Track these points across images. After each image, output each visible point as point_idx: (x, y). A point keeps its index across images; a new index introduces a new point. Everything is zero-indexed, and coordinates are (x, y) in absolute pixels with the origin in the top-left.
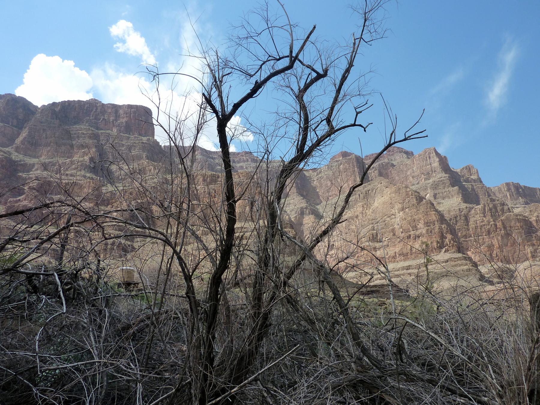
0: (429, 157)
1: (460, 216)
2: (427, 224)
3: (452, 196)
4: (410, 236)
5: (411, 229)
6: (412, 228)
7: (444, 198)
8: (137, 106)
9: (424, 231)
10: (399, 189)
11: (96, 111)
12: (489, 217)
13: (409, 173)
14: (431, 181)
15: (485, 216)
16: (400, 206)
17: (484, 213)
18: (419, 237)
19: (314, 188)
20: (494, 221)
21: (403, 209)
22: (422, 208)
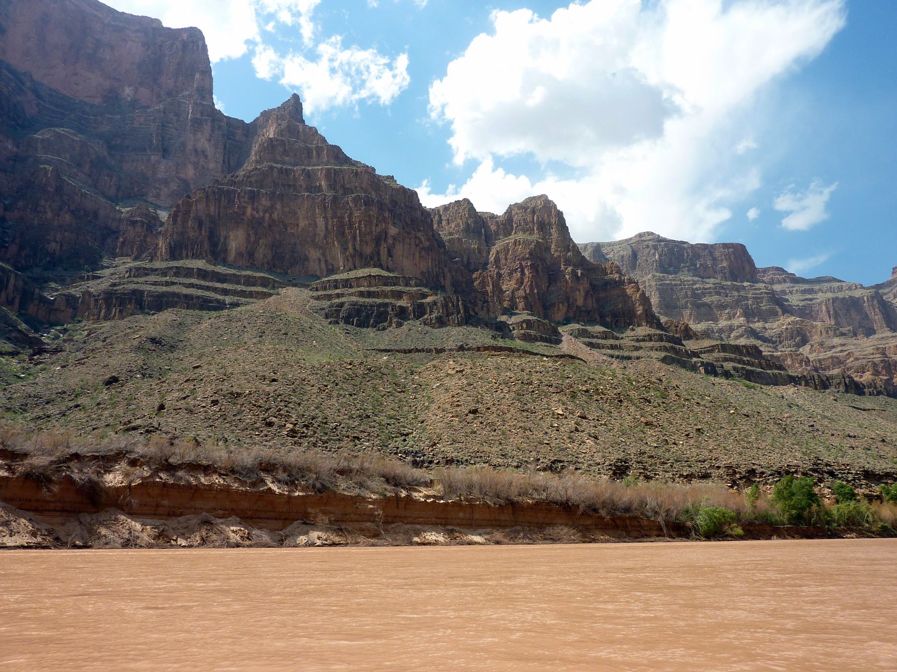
8: (732, 244)
11: (688, 255)
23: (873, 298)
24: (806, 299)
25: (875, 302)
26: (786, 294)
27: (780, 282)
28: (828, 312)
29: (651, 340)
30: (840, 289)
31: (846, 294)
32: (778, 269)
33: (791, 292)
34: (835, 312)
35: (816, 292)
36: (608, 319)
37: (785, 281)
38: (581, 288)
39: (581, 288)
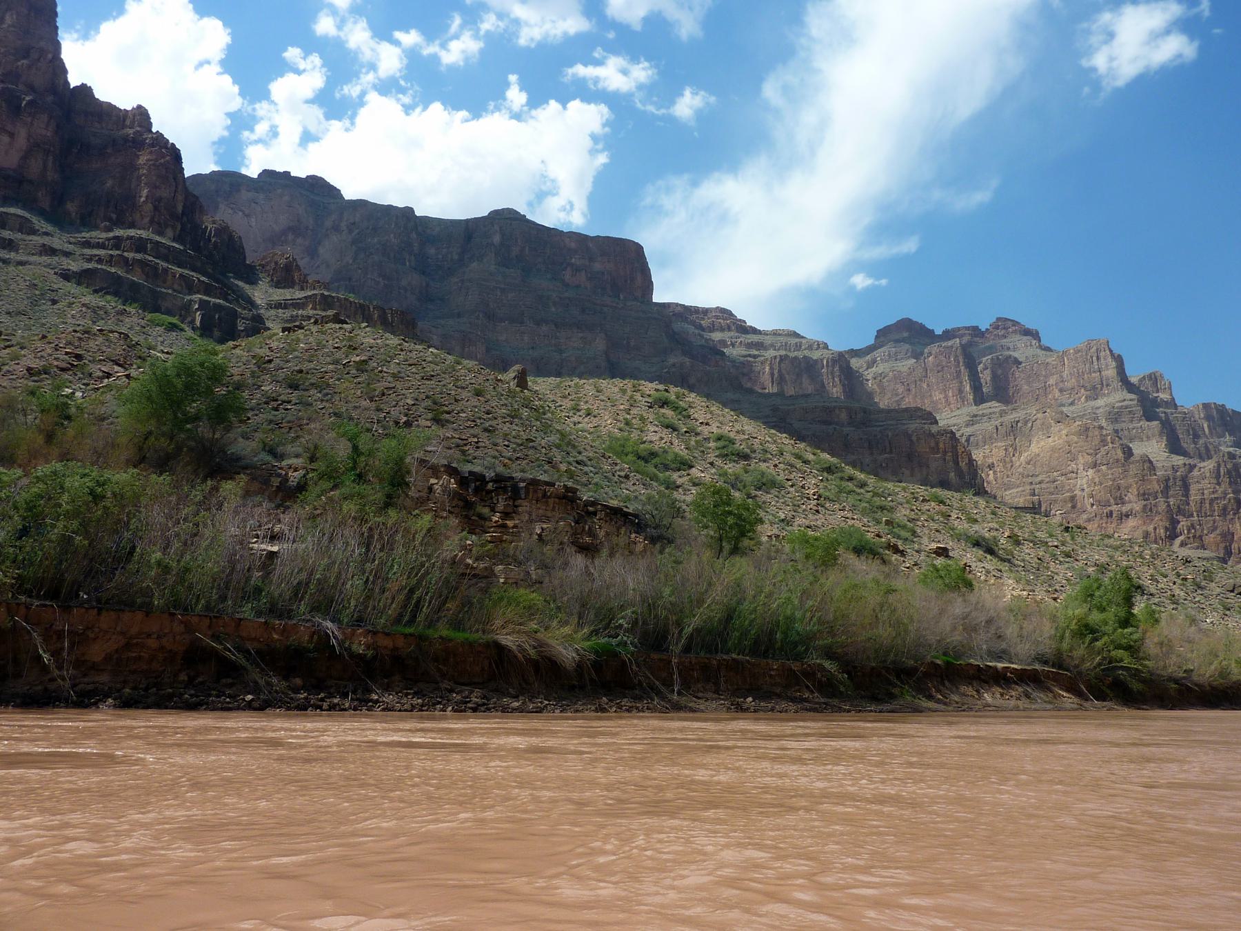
0: (1098, 358)
1: (1174, 479)
2: (1144, 496)
3: (1148, 438)
4: (1111, 512)
5: (1112, 501)
6: (1115, 499)
7: (1131, 440)
9: (1137, 507)
10: (1087, 429)
12: (1225, 486)
13: (1052, 381)
14: (1100, 402)
15: (1219, 484)
16: (1090, 459)
17: (1218, 476)
18: (1127, 516)
19: (870, 395)
20: (1233, 492)
21: (1095, 465)
22: (1133, 469)
23: (834, 361)
24: (750, 356)
25: (837, 368)
26: (727, 346)
27: (722, 330)
28: (772, 374)
29: (117, 247)
30: (798, 347)
31: (800, 354)
32: (723, 311)
33: (733, 345)
34: (781, 377)
35: (766, 349)
36: (71, 207)
37: (729, 329)
38: (22, 133)
39: (22, 133)
